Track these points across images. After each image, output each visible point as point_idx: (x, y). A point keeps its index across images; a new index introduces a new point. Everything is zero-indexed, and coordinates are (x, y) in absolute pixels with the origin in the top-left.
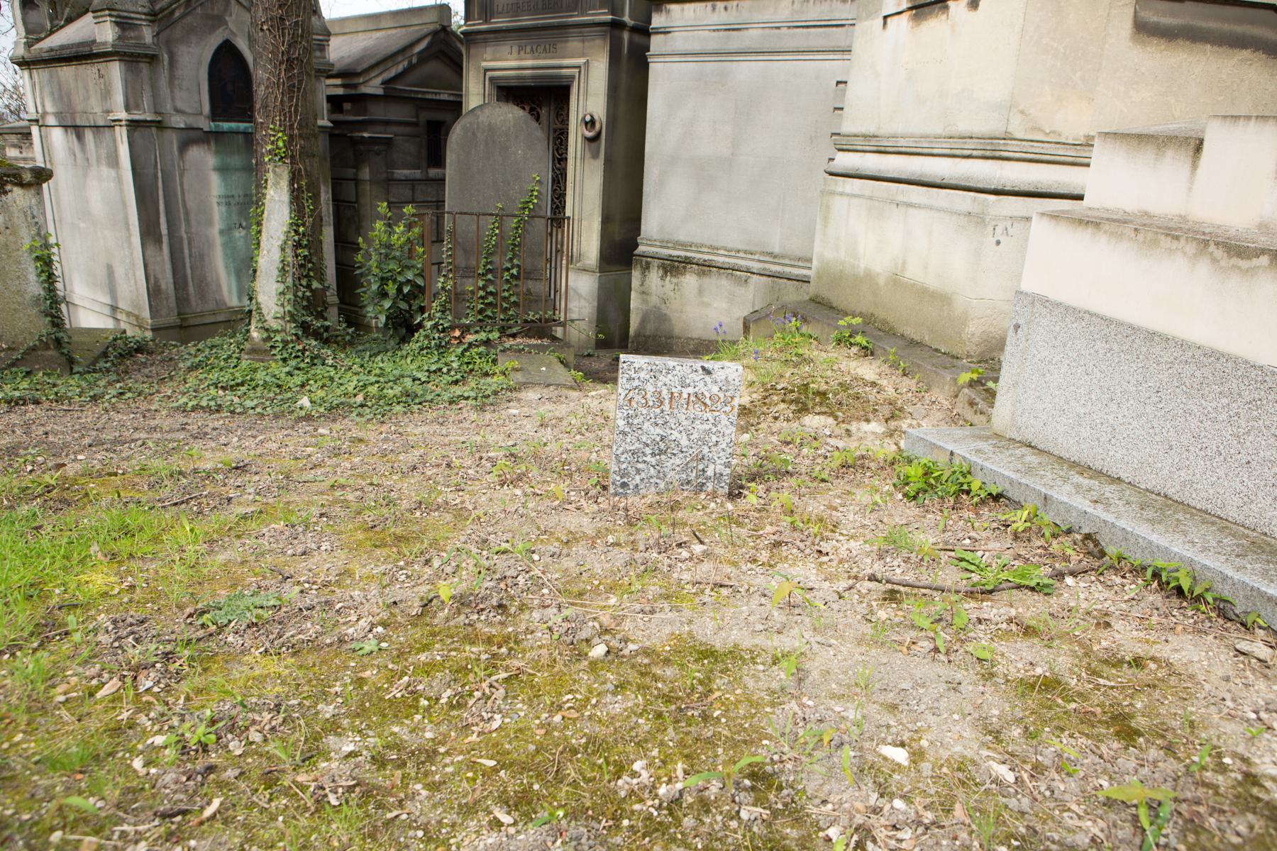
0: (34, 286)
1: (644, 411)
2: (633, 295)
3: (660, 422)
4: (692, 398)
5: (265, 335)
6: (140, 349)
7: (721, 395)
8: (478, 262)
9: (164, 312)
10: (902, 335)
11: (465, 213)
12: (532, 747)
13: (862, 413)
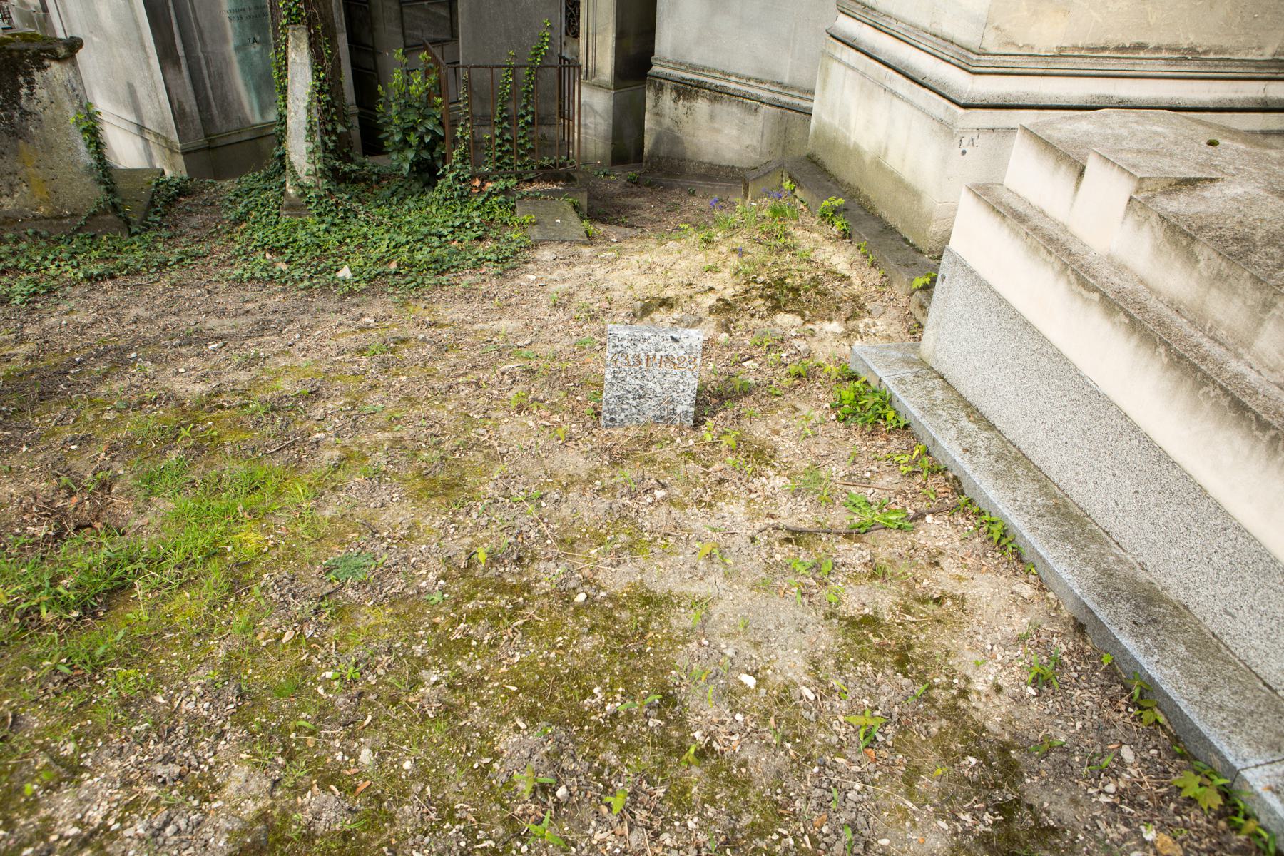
0: (85, 157)
1: (627, 369)
2: (647, 115)
3: (639, 376)
4: (664, 359)
5: (300, 192)
6: (183, 191)
7: (687, 356)
8: (494, 110)
9: (191, 135)
10: (880, 216)
11: (479, 67)
12: (537, 677)
13: (827, 312)
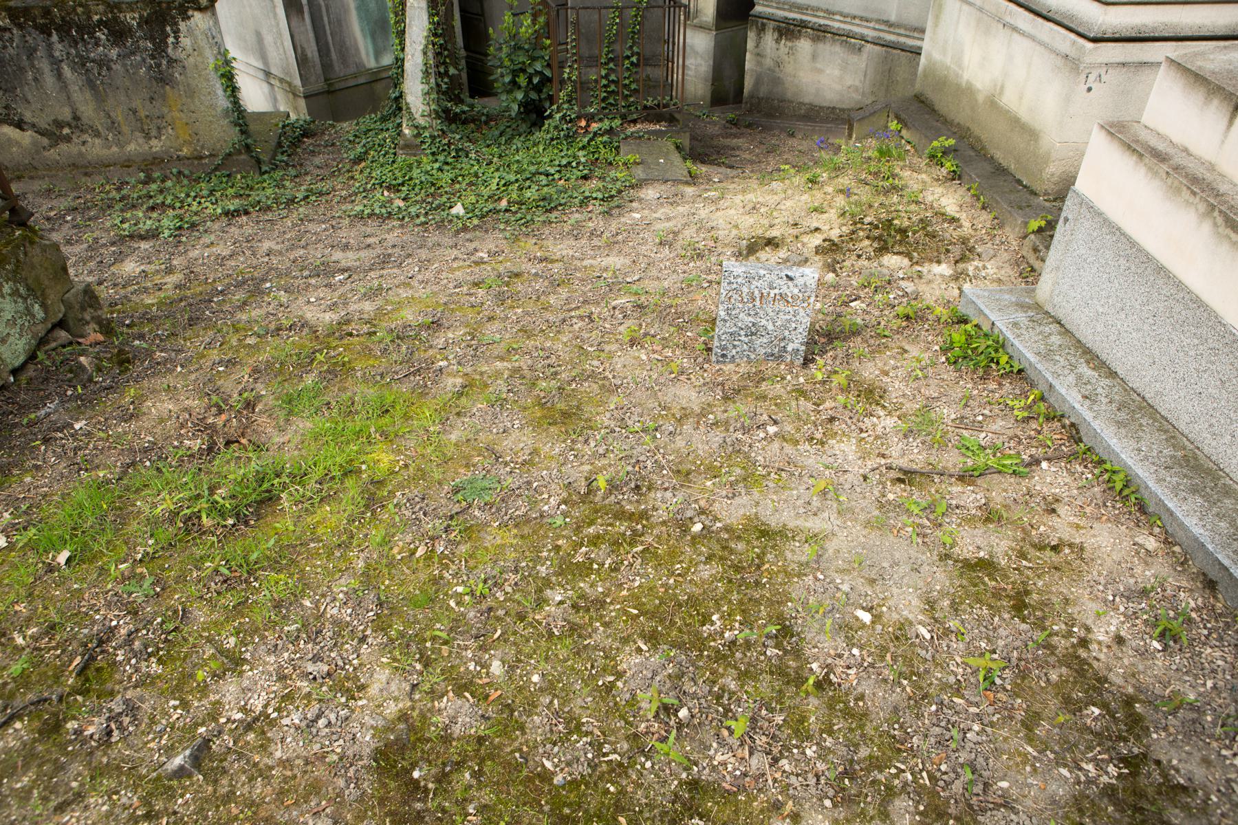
0: (223, 102)
1: (740, 306)
2: (748, 56)
3: (752, 313)
4: (778, 297)
5: (416, 132)
6: (306, 133)
7: (800, 295)
8: (601, 51)
9: (313, 79)
10: (992, 157)
11: (588, 8)
12: (657, 602)
13: (936, 254)
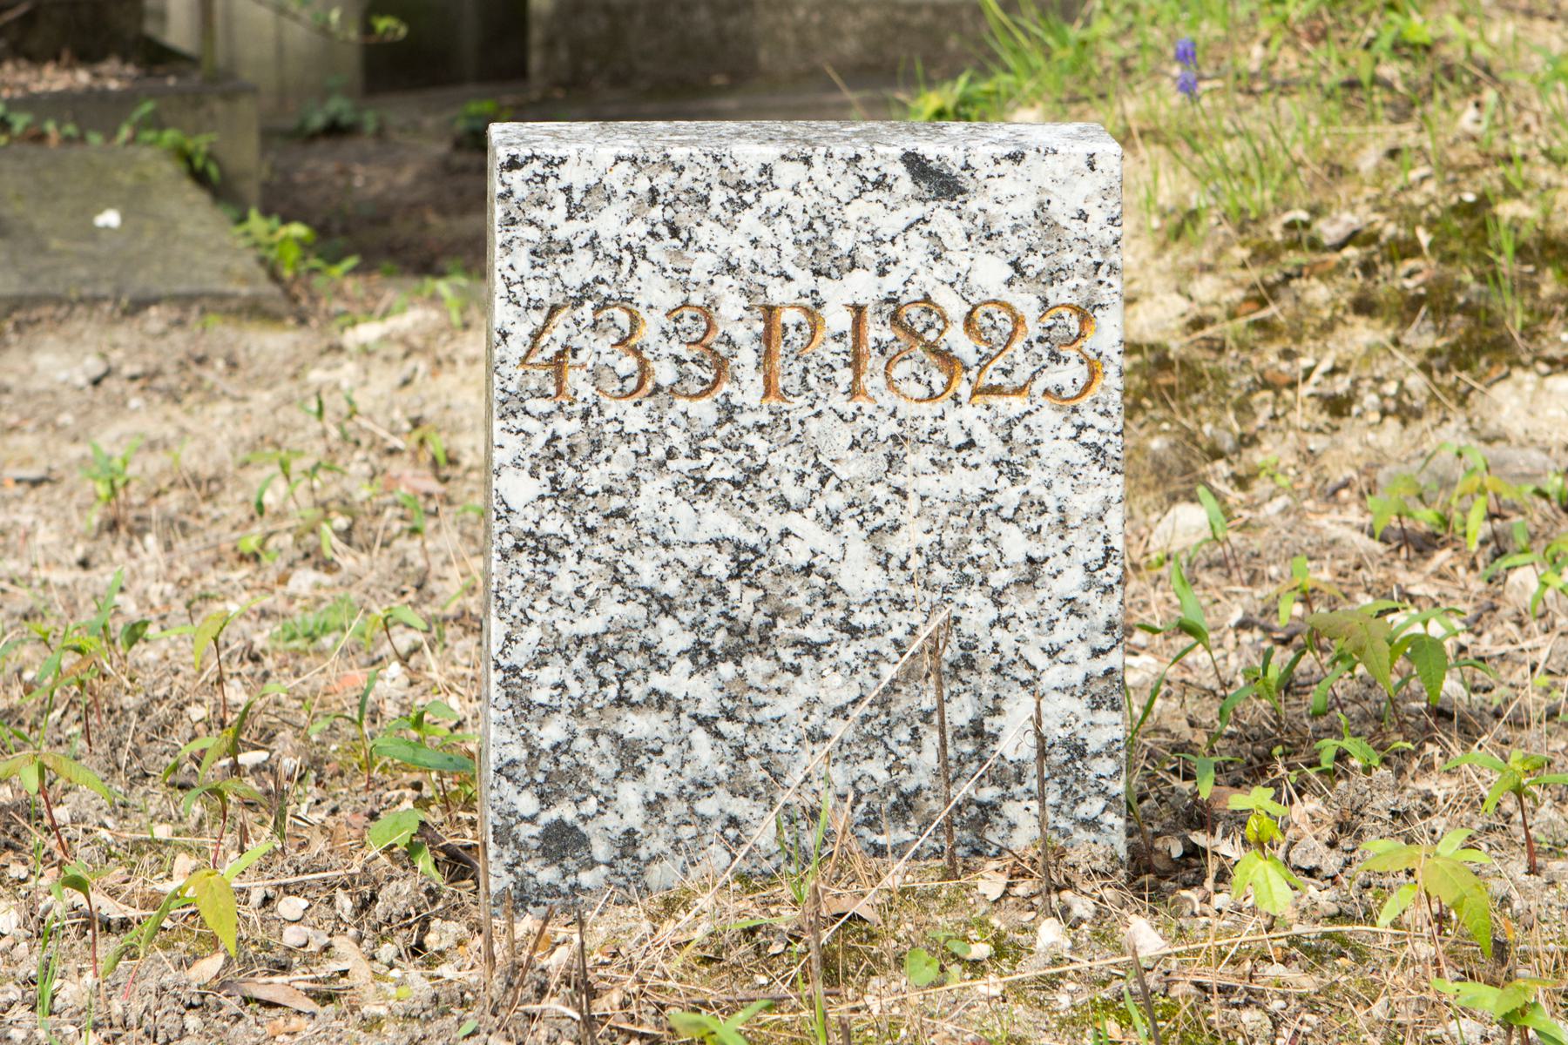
1: (636, 420)
3: (722, 470)
4: (878, 332)
7: (1025, 301)
